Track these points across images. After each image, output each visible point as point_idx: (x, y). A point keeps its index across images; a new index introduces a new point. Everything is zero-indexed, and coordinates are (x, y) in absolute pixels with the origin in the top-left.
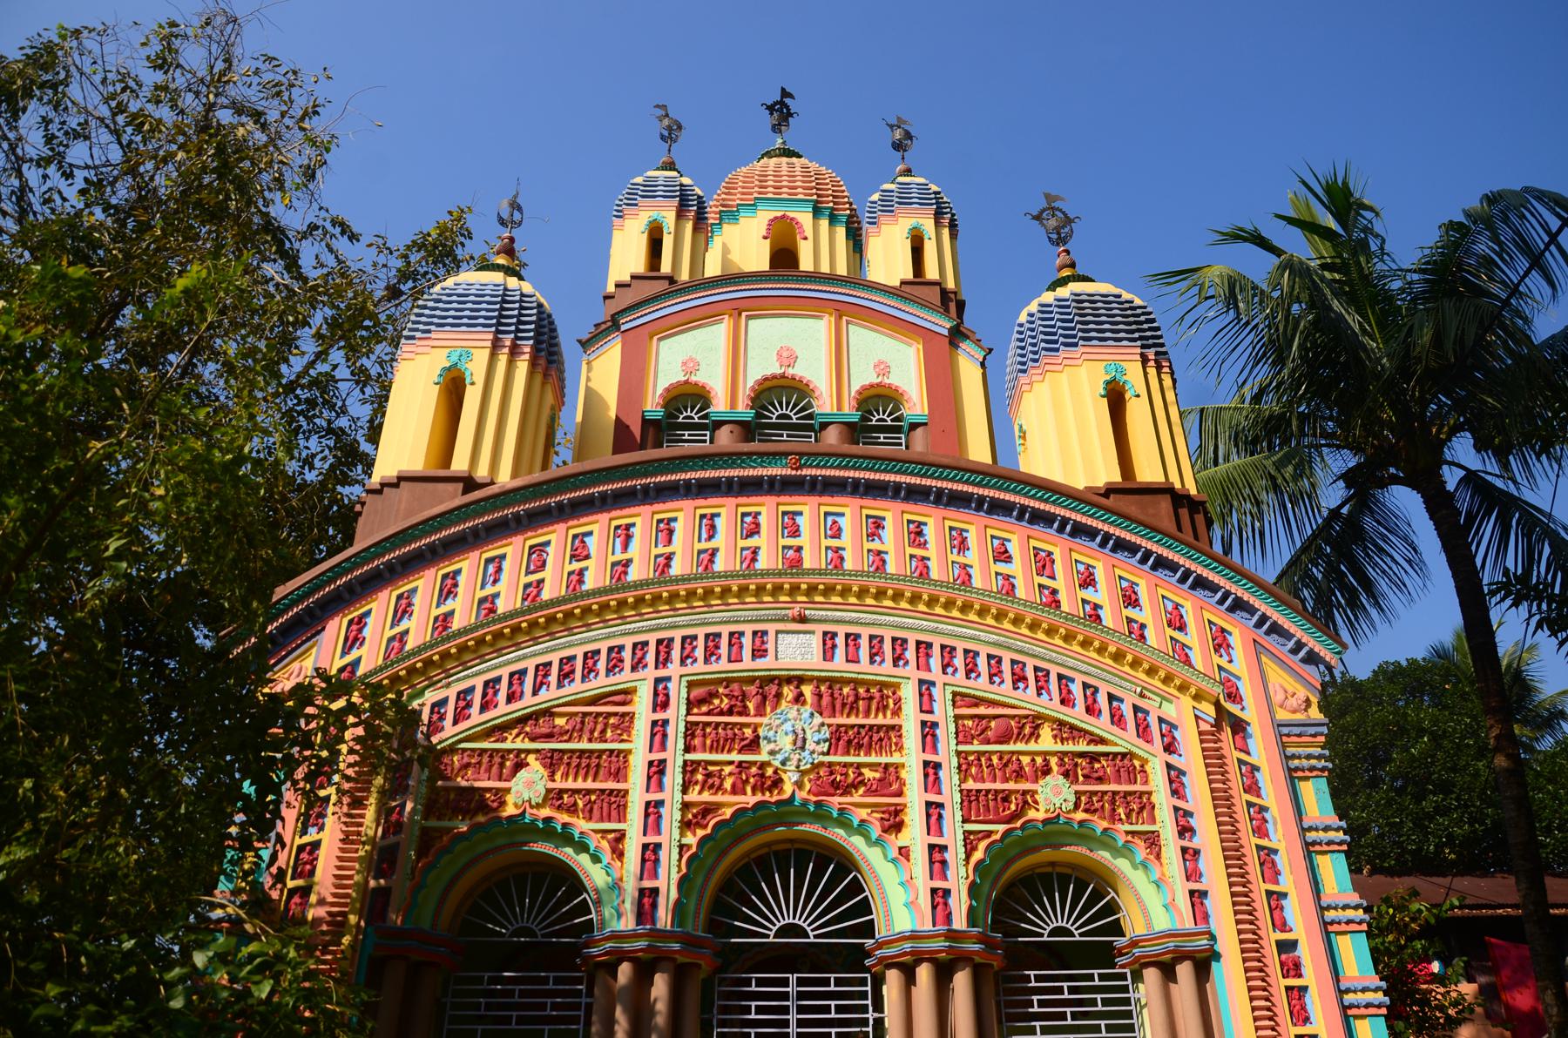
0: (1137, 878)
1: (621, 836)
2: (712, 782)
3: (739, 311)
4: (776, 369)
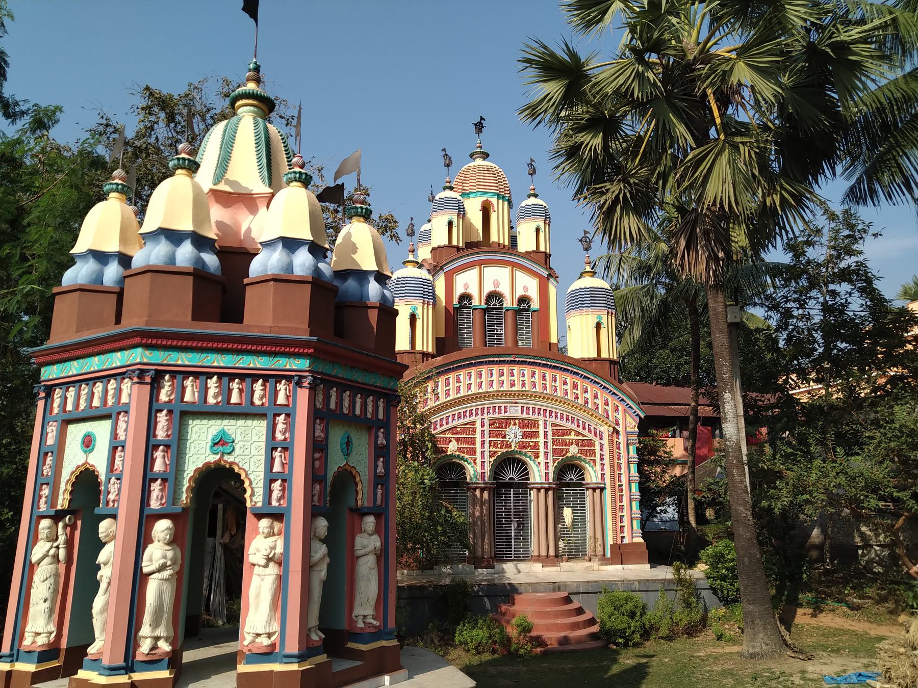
0: (590, 469)
1: (476, 459)
2: (495, 446)
3: (481, 263)
4: (492, 289)
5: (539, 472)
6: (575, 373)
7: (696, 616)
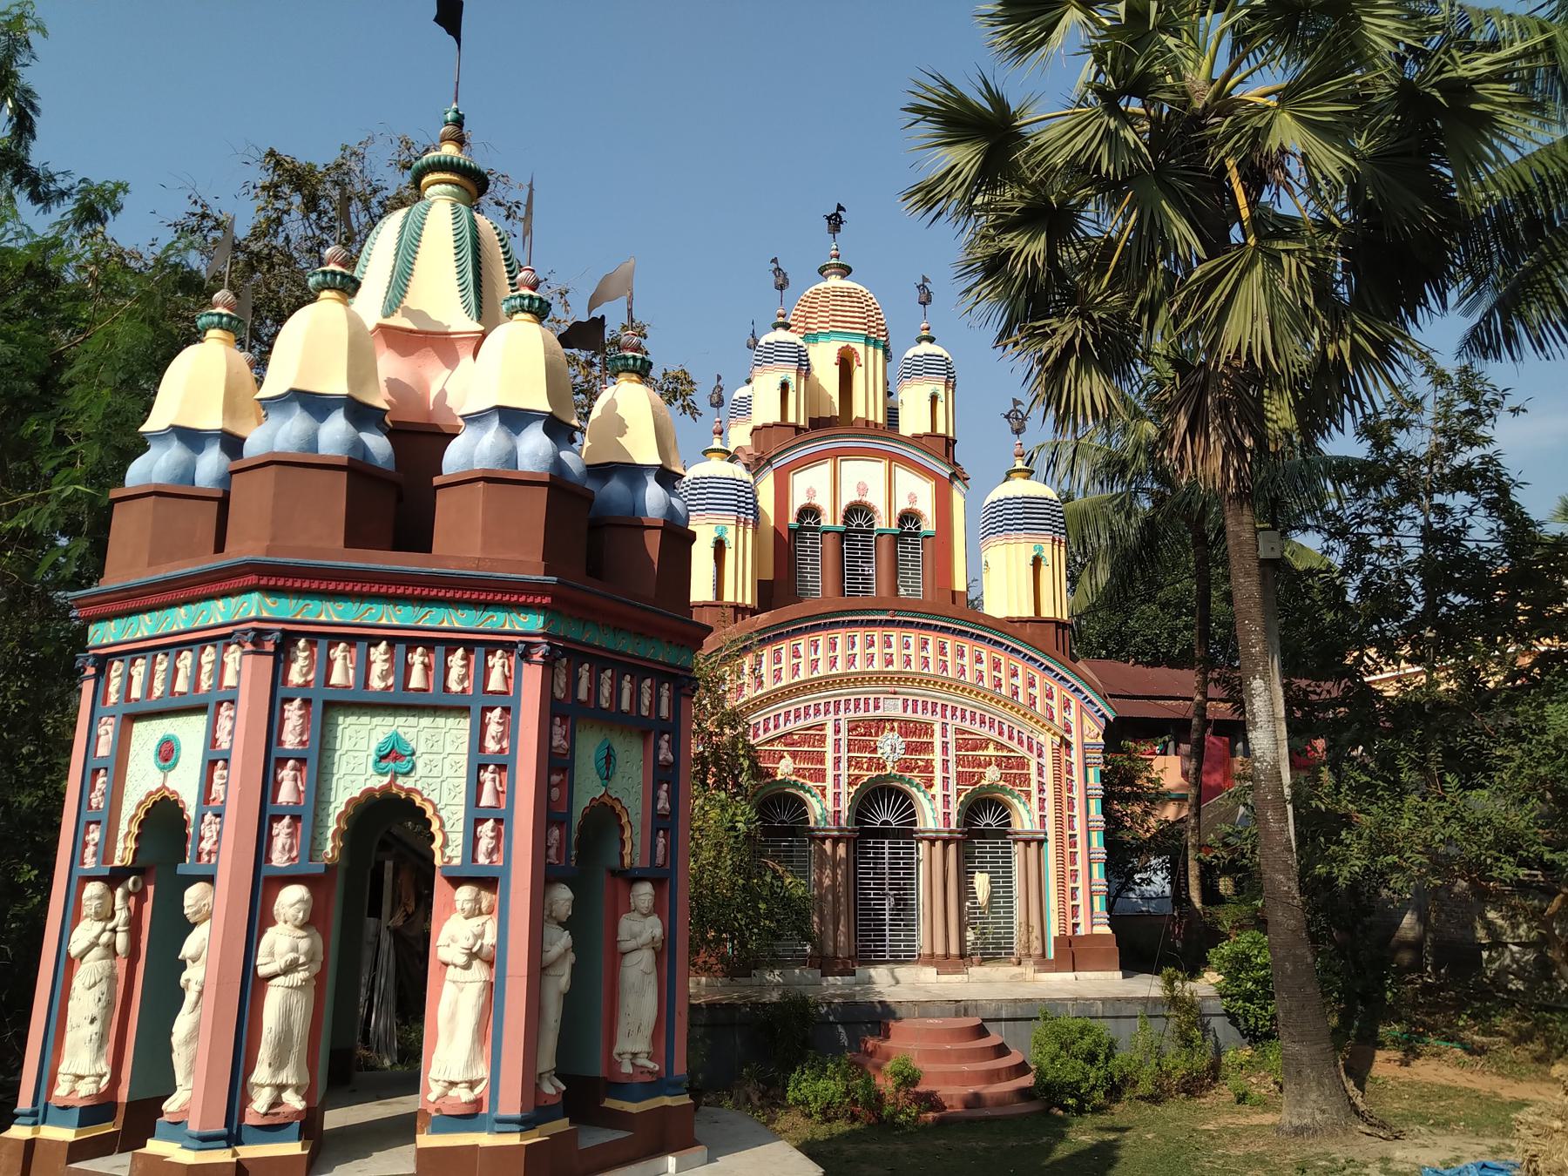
0: (1020, 807)
1: (825, 788)
2: (859, 766)
3: (837, 455)
5: (934, 811)
6: (996, 643)
7: (1201, 1062)
